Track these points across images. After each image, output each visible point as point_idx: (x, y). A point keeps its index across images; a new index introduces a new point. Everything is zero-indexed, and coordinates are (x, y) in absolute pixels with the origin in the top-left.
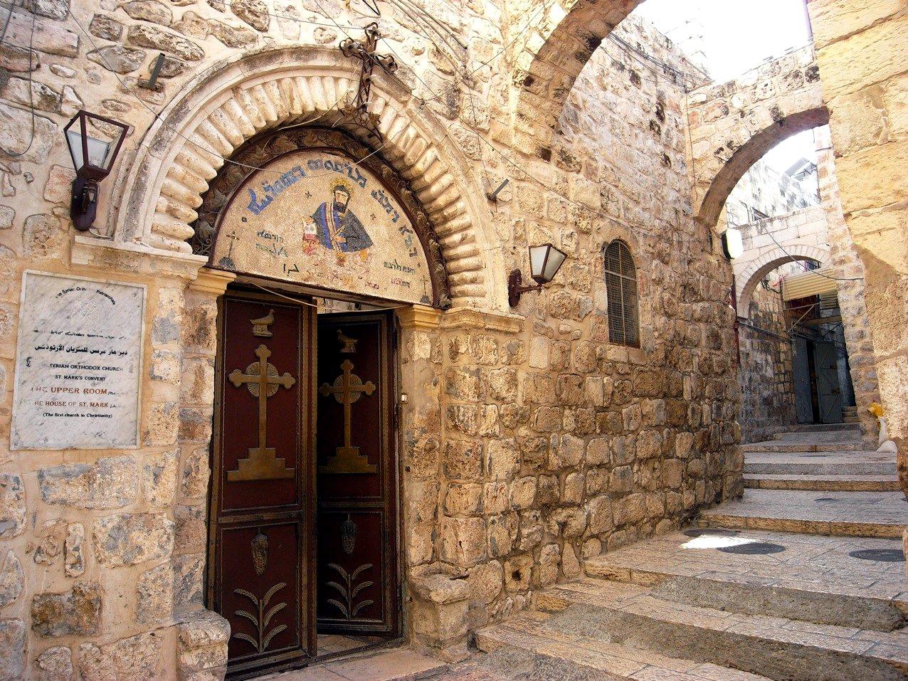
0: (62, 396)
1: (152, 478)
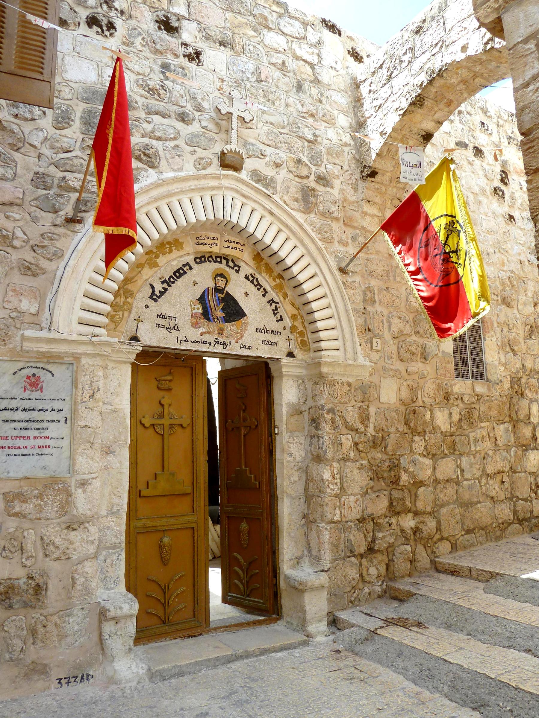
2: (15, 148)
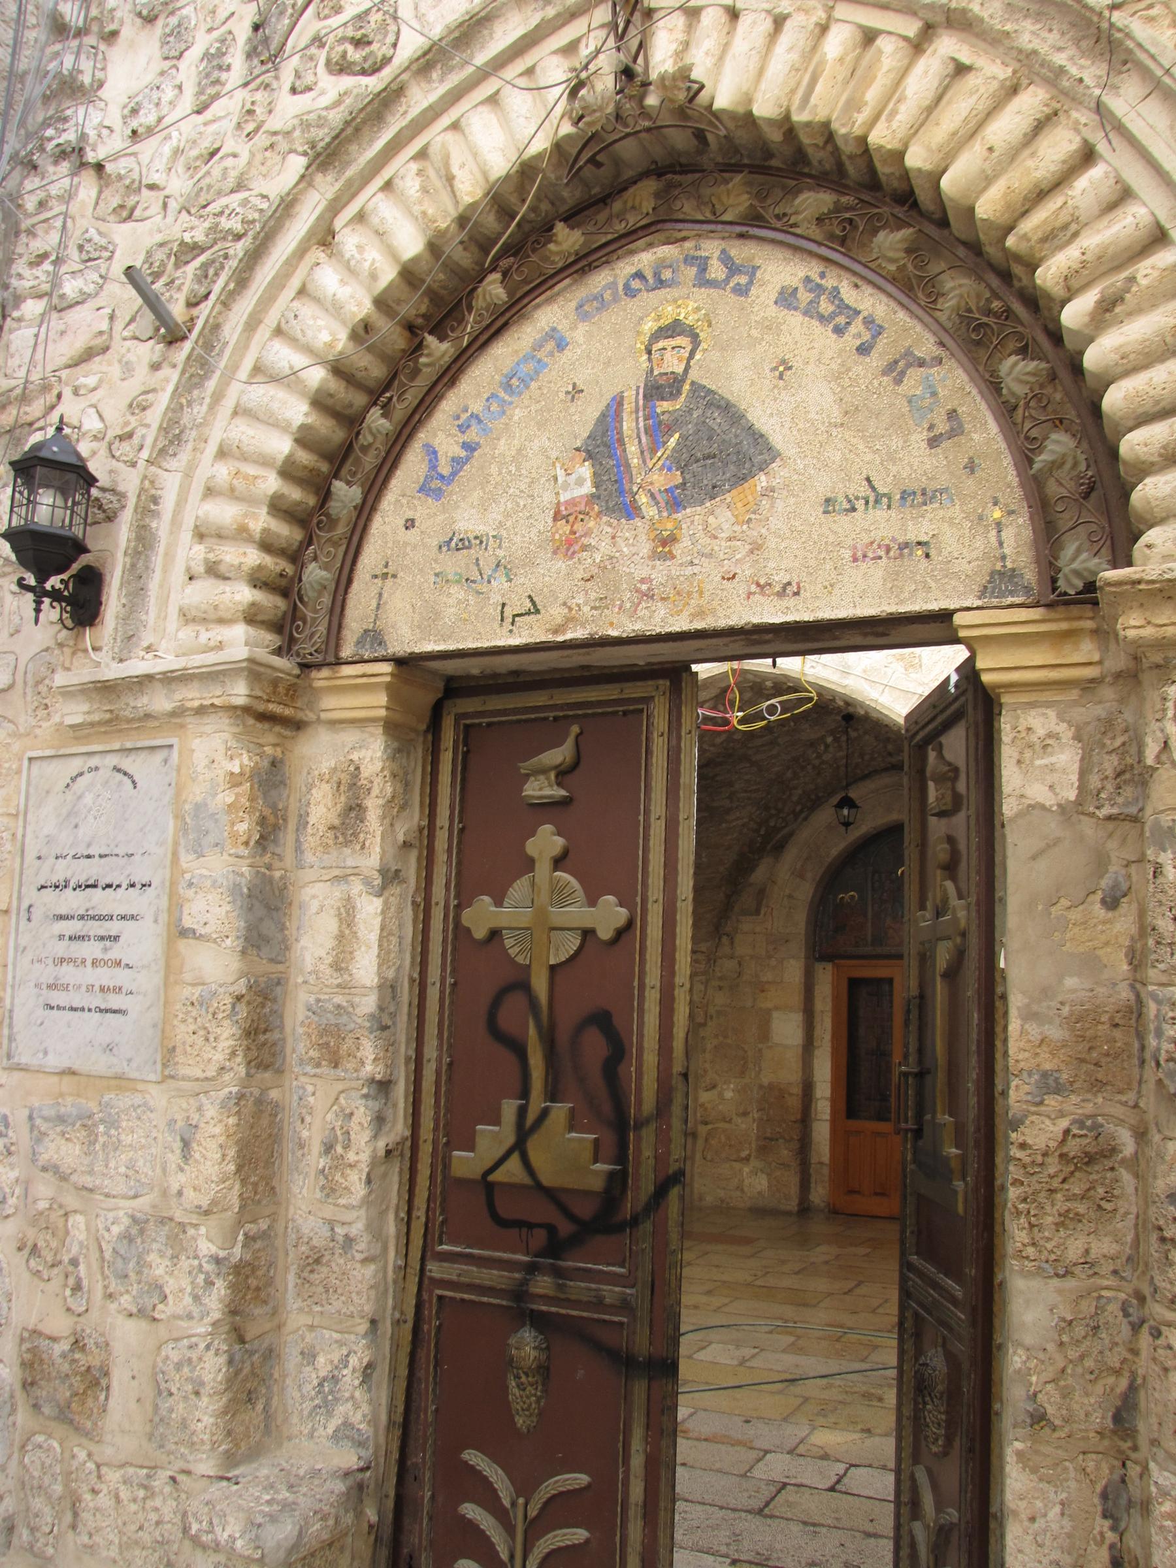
0: (68, 973)
1: (177, 1145)
2: (125, 214)
